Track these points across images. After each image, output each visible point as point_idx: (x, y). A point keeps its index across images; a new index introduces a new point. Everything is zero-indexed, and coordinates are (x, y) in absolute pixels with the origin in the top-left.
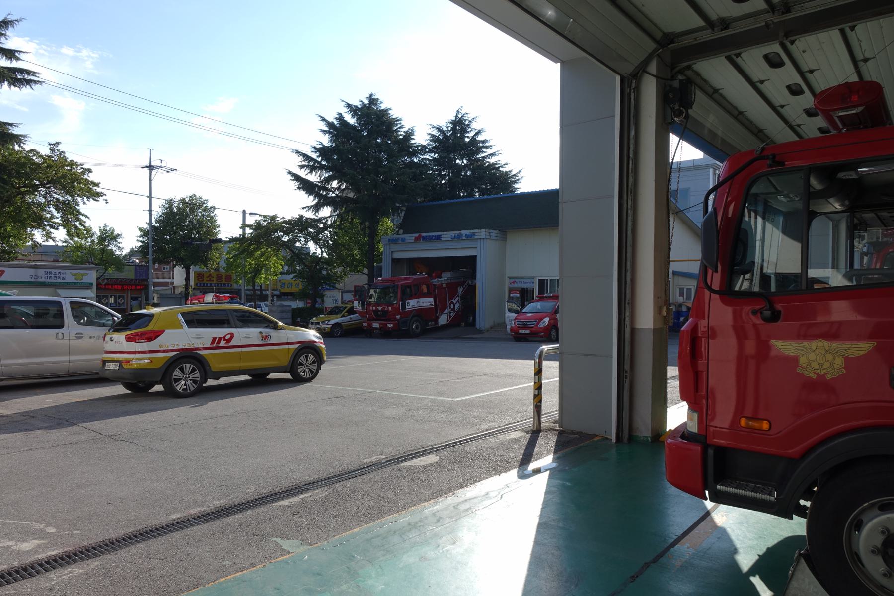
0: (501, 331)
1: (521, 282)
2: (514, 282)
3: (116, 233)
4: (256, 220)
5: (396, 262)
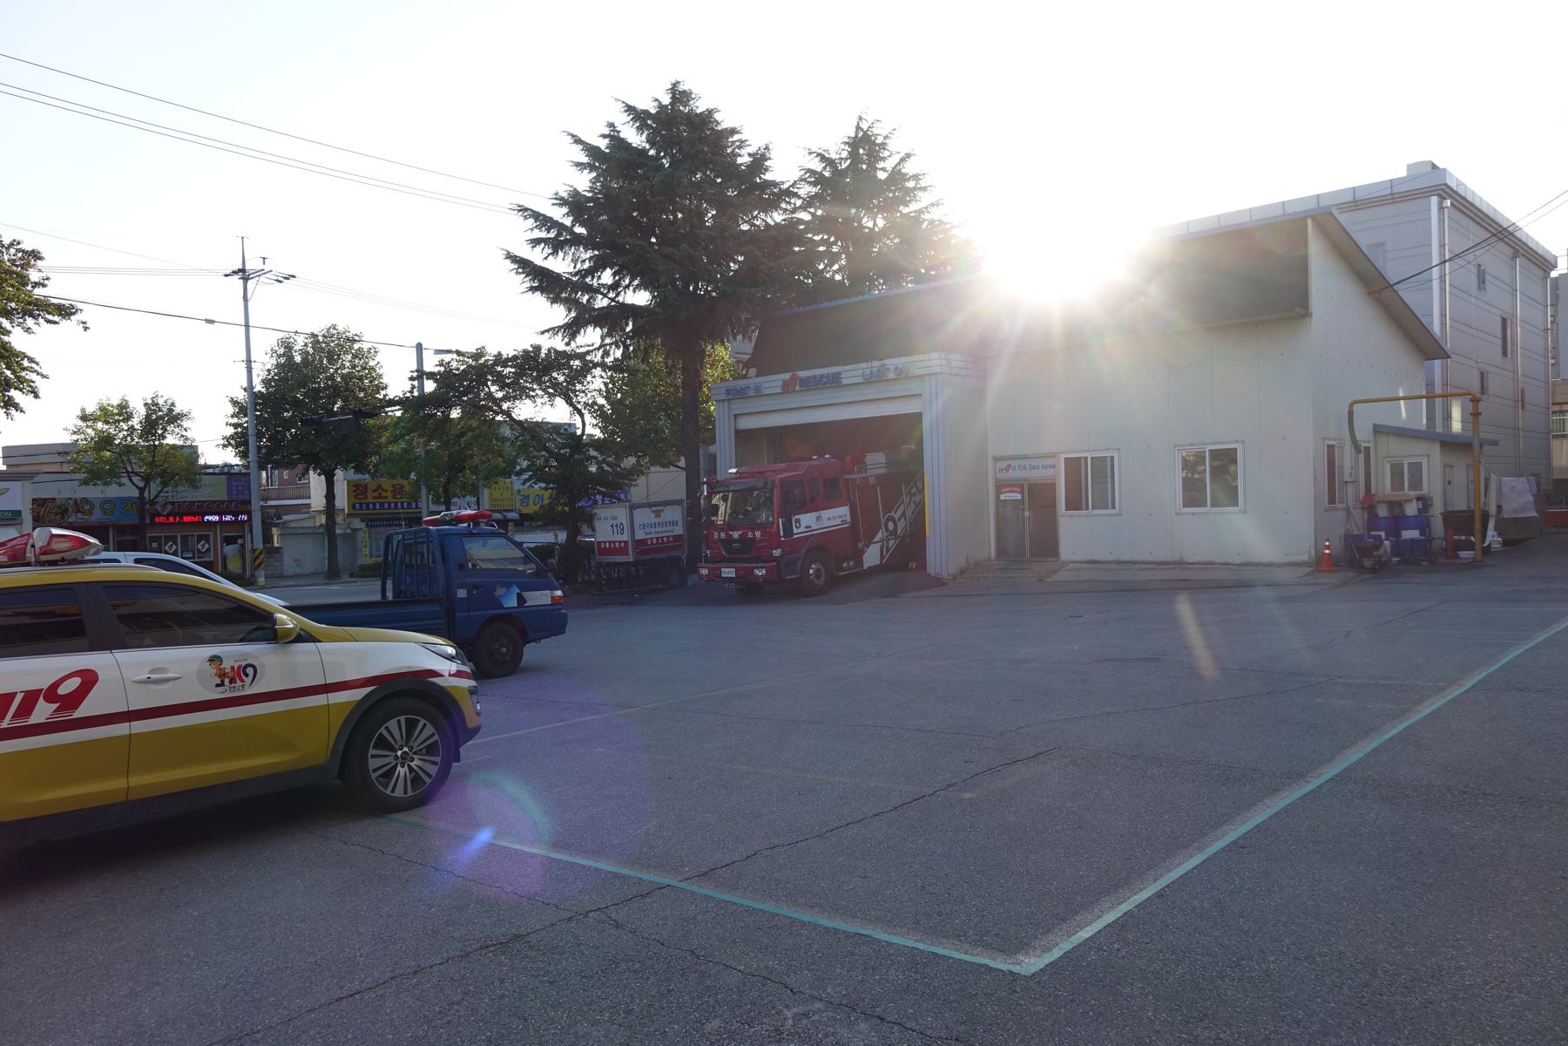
0: (986, 578)
1: (1025, 468)
2: (1007, 468)
3: (177, 410)
4: (442, 360)
5: (744, 437)
